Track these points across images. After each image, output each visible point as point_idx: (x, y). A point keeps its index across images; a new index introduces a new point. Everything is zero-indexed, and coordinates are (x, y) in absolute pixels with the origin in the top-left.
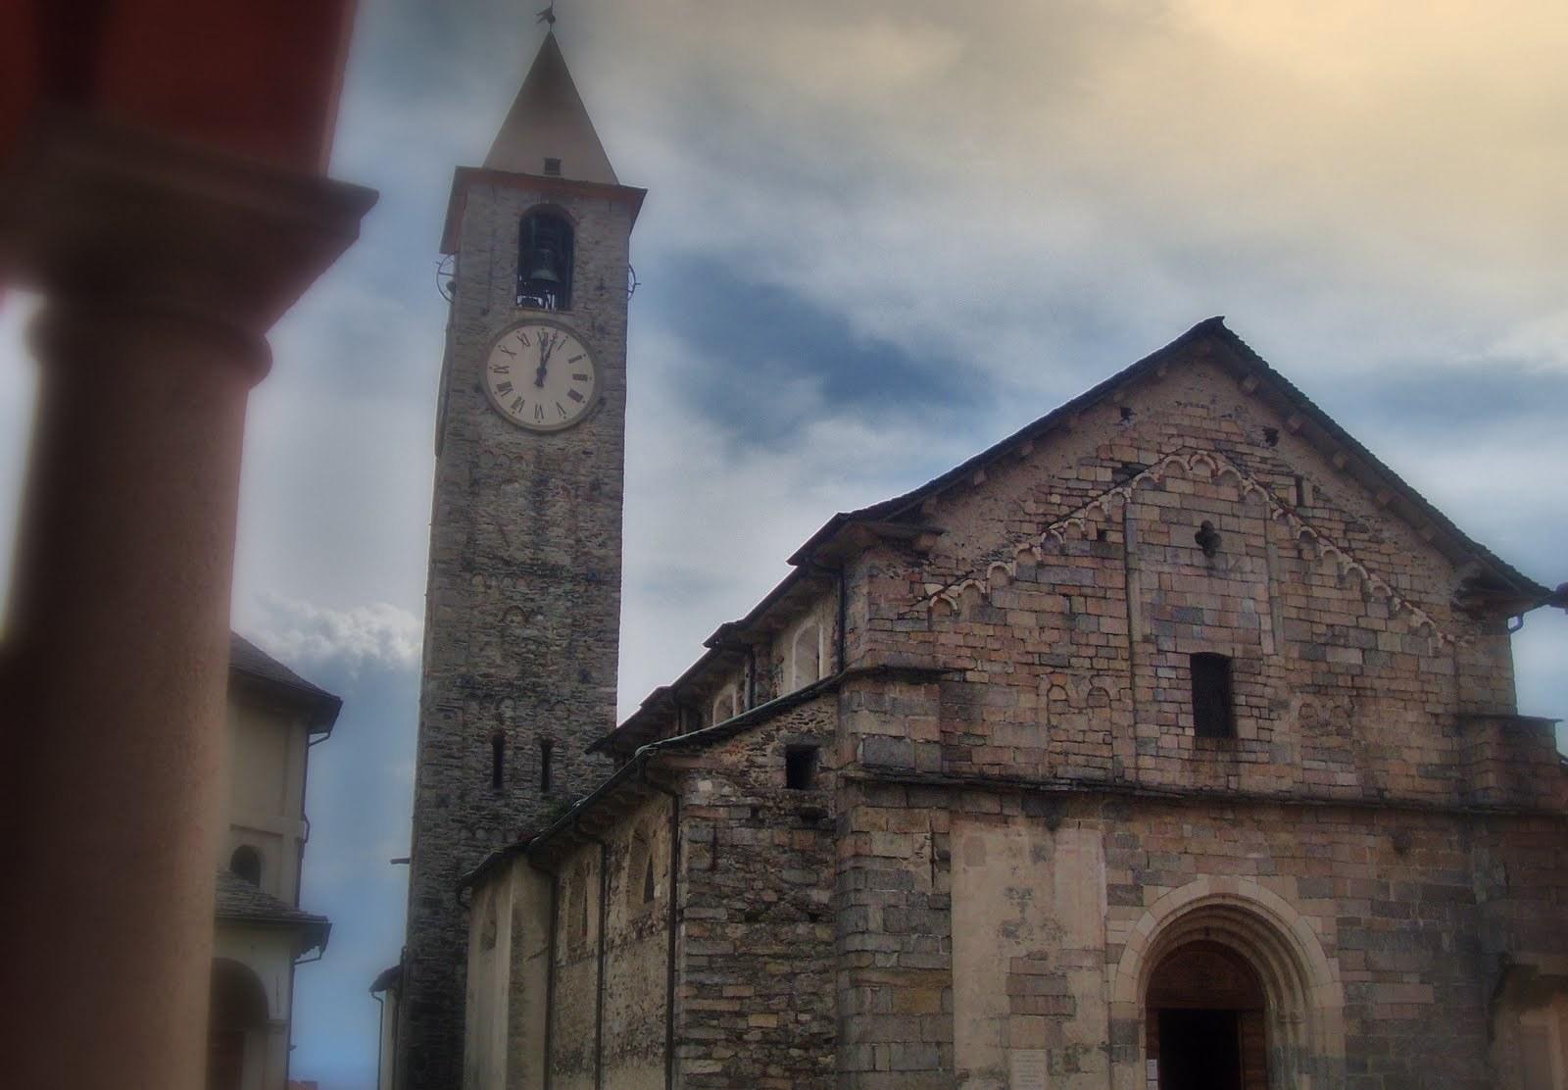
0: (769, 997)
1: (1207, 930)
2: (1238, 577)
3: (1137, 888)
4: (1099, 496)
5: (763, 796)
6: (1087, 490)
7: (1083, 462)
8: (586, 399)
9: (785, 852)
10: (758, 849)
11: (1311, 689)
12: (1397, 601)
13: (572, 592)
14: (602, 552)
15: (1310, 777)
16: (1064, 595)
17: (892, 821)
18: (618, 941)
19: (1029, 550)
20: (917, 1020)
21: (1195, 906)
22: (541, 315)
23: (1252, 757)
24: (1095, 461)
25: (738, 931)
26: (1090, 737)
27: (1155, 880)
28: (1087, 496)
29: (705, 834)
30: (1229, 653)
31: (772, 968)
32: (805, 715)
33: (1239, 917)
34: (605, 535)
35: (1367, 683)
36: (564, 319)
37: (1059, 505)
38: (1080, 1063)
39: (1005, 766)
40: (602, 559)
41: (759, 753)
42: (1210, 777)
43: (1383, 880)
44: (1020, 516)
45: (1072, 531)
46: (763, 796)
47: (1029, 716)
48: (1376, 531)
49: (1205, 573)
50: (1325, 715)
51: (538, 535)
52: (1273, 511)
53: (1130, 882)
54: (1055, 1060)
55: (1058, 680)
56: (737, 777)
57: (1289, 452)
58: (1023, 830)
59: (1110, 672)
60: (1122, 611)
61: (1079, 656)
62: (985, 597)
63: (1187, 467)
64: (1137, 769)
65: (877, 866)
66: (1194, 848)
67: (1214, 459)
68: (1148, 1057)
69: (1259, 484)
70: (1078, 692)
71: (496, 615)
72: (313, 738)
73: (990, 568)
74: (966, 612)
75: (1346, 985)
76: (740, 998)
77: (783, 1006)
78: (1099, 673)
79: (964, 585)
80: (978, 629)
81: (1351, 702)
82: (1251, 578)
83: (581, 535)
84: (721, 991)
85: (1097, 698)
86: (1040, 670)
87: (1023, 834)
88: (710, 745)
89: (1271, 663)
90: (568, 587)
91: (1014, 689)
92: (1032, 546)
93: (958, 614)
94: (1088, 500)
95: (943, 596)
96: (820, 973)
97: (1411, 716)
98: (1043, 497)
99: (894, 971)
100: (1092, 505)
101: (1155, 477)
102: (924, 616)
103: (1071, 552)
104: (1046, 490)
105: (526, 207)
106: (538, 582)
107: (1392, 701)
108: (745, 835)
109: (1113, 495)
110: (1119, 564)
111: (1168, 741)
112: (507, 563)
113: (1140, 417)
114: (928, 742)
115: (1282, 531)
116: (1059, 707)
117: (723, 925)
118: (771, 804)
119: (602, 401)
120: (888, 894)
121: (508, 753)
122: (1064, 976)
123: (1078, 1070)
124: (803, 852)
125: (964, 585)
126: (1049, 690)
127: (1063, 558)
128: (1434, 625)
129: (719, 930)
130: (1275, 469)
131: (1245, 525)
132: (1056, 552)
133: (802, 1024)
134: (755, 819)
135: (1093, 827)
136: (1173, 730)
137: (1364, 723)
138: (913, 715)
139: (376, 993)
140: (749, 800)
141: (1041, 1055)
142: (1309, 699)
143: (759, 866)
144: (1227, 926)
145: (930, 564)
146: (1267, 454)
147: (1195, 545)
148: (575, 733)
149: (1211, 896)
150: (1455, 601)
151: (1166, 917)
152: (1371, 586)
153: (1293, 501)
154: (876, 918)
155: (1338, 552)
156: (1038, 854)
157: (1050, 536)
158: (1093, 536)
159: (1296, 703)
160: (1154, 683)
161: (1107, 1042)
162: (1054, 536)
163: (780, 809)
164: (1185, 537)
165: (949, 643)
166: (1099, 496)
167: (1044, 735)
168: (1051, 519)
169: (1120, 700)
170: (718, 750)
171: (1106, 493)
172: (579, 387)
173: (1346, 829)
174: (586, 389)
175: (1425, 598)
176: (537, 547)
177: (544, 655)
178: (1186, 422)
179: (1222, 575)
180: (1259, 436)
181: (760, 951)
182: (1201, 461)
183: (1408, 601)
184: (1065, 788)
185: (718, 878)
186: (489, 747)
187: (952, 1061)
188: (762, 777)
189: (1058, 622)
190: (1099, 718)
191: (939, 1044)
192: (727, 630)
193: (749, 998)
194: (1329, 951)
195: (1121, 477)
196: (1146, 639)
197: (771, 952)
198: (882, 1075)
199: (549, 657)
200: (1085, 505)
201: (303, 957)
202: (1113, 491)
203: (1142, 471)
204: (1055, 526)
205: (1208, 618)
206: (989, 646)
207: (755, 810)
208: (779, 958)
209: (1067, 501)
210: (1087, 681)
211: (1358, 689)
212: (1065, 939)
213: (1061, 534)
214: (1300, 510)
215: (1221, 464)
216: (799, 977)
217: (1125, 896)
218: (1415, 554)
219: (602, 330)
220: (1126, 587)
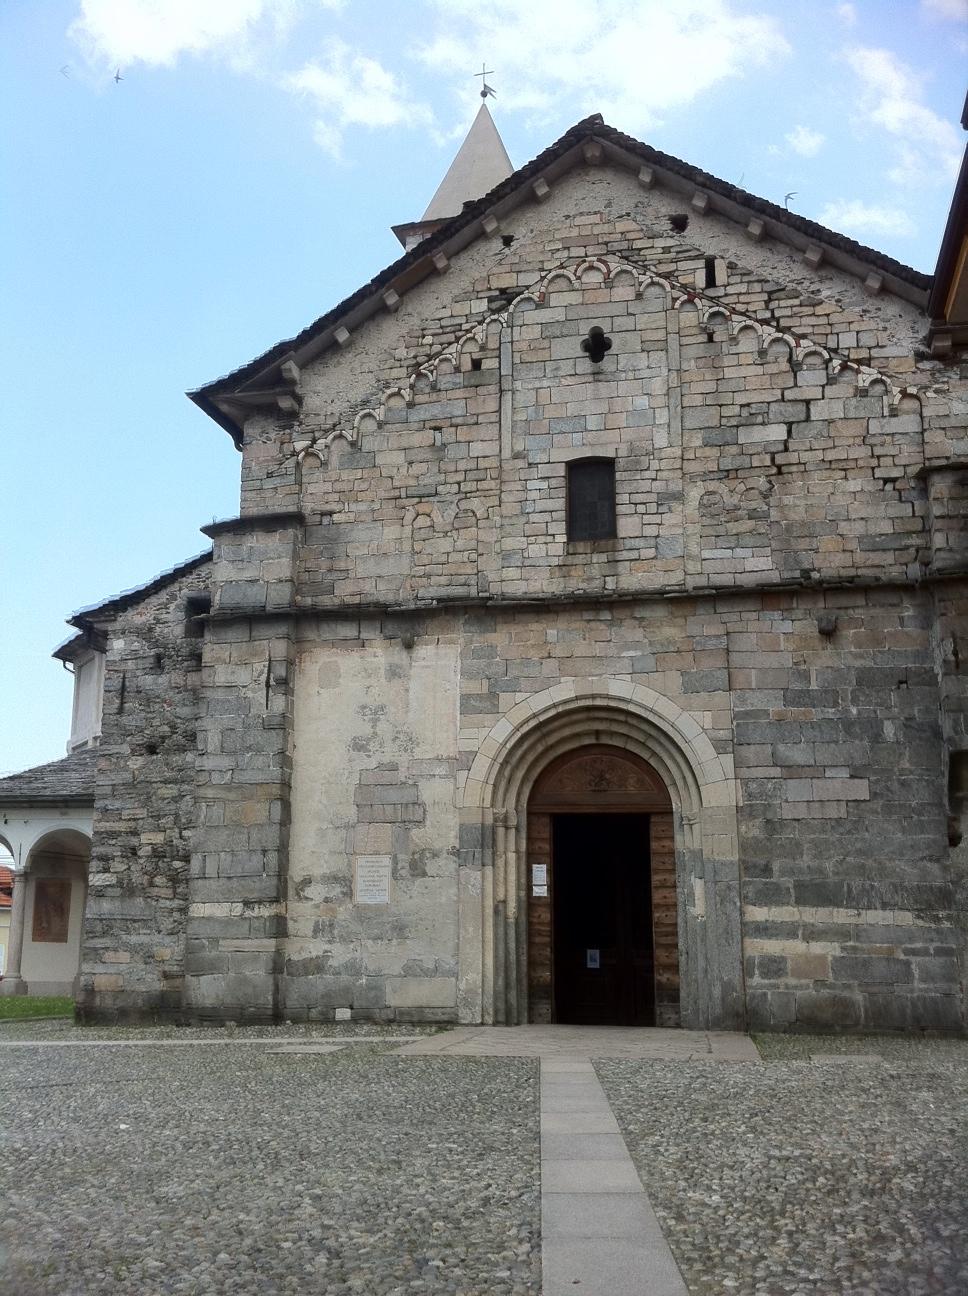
1: (597, 733)
2: (631, 375)
3: (493, 695)
4: (473, 328)
6: (461, 325)
7: (458, 299)
11: (716, 476)
12: (836, 363)
15: (709, 567)
17: (234, 654)
19: (398, 394)
20: (246, 831)
23: (634, 555)
24: (473, 294)
25: (135, 763)
26: (454, 557)
28: (461, 330)
30: (611, 454)
33: (622, 718)
35: (793, 457)
37: (431, 345)
38: (427, 869)
41: (164, 611)
42: (591, 574)
43: (803, 667)
45: (445, 367)
47: (392, 548)
48: (813, 292)
49: (591, 379)
50: (731, 501)
52: (675, 300)
53: (485, 690)
55: (422, 508)
56: (146, 633)
57: (702, 236)
58: (379, 652)
61: (446, 483)
62: (353, 444)
63: (573, 278)
65: (220, 695)
66: (558, 652)
67: (604, 262)
69: (659, 275)
73: (358, 418)
75: (746, 782)
78: (467, 495)
79: (331, 437)
81: (770, 482)
82: (646, 373)
84: (120, 814)
86: (405, 502)
87: (380, 653)
88: (125, 610)
89: (663, 455)
91: (379, 523)
92: (400, 389)
93: (324, 464)
94: (460, 334)
97: (853, 485)
99: (228, 787)
100: (464, 338)
103: (442, 388)
104: (419, 333)
107: (826, 474)
108: (147, 681)
109: (488, 324)
110: (493, 389)
111: (536, 550)
113: (522, 241)
115: (689, 318)
116: (423, 534)
117: (126, 758)
120: (227, 720)
122: (415, 785)
123: (424, 874)
127: (434, 395)
128: (888, 381)
129: (122, 763)
130: (680, 255)
131: (642, 321)
132: (427, 390)
133: (185, 840)
135: (452, 642)
136: (542, 539)
137: (786, 502)
138: (268, 559)
141: (387, 861)
142: (712, 486)
143: (157, 706)
144: (615, 728)
145: (301, 424)
146: (670, 242)
147: (582, 354)
149: (577, 698)
150: (922, 348)
152: (799, 354)
153: (700, 279)
155: (757, 325)
156: (394, 672)
157: (420, 375)
158: (467, 365)
159: (695, 493)
160: (521, 496)
161: (458, 846)
164: (573, 347)
165: (317, 493)
166: (473, 328)
167: (406, 561)
168: (420, 359)
169: (488, 518)
171: (480, 323)
173: (754, 615)
175: (875, 353)
178: (575, 233)
179: (610, 377)
180: (666, 226)
182: (591, 268)
183: (852, 361)
185: (125, 720)
189: (428, 455)
190: (464, 539)
193: (143, 819)
194: (720, 747)
195: (495, 305)
198: (211, 881)
200: (457, 339)
203: (522, 293)
204: (426, 365)
205: (592, 423)
207: (159, 658)
208: (170, 783)
209: (438, 339)
210: (454, 506)
211: (779, 467)
212: (417, 750)
213: (432, 372)
214: (711, 292)
215: (612, 266)
216: (185, 799)
217: (479, 704)
218: (865, 307)
220: (499, 411)
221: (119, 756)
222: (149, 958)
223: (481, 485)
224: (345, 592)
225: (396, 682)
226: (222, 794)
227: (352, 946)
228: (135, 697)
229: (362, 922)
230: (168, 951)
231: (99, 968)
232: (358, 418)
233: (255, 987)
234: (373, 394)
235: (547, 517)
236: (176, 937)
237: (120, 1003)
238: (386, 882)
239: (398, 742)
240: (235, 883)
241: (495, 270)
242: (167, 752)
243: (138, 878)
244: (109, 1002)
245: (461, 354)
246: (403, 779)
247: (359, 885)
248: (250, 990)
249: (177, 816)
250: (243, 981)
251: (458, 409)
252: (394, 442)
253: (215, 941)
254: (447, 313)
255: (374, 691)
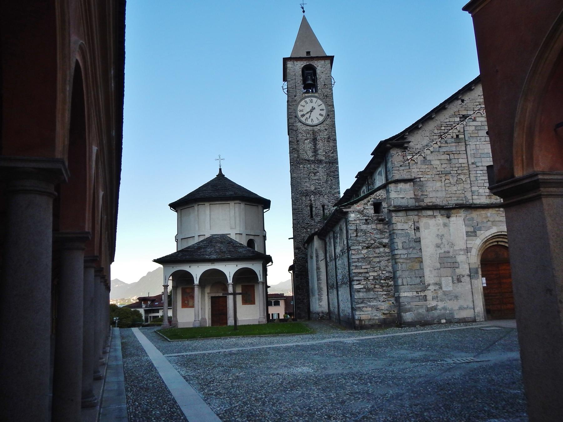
0: (374, 268)
1: (497, 242)
5: (368, 216)
8: (324, 115)
9: (375, 230)
10: (368, 230)
13: (326, 166)
14: (333, 155)
16: (448, 154)
18: (338, 256)
19: (436, 143)
21: (493, 235)
22: (310, 95)
24: (455, 115)
25: (364, 251)
26: (458, 192)
27: (480, 229)
29: (353, 227)
31: (374, 260)
32: (378, 194)
34: (333, 150)
36: (316, 95)
37: (444, 130)
38: (462, 280)
39: (434, 202)
40: (333, 157)
44: (433, 134)
45: (449, 136)
46: (368, 216)
47: (440, 189)
51: (315, 153)
54: (454, 280)
55: (447, 177)
59: (462, 174)
60: (465, 156)
62: (424, 158)
64: (472, 199)
65: (400, 232)
68: (482, 277)
70: (453, 180)
71: (307, 174)
72: (265, 211)
73: (425, 150)
74: (419, 163)
76: (367, 268)
77: (378, 270)
78: (459, 174)
79: (418, 155)
80: (423, 166)
83: (327, 151)
85: (459, 181)
86: (441, 175)
87: (440, 220)
90: (325, 165)
91: (434, 181)
92: (437, 142)
93: (417, 163)
95: (412, 159)
96: (387, 260)
98: (439, 128)
99: (406, 259)
101: (473, 118)
102: (408, 165)
103: (448, 142)
105: (303, 66)
106: (317, 165)
108: (364, 227)
110: (463, 144)
111: (481, 191)
112: (308, 161)
113: (467, 101)
114: (411, 198)
116: (448, 185)
117: (361, 250)
118: (370, 218)
119: (328, 115)
120: (403, 239)
121: (314, 209)
122: (455, 257)
123: (461, 282)
124: (380, 230)
125: (418, 155)
126: (445, 181)
127: (446, 144)
129: (360, 252)
132: (444, 143)
134: (367, 222)
135: (460, 216)
136: (483, 188)
139: (290, 272)
140: (365, 218)
141: (450, 278)
143: (368, 234)
145: (408, 151)
147: (487, 135)
148: (330, 202)
149: (497, 232)
151: (484, 239)
154: (400, 246)
156: (445, 225)
157: (442, 138)
160: (476, 175)
162: (443, 138)
163: (373, 219)
165: (415, 172)
167: (444, 193)
168: (442, 134)
169: (466, 181)
170: (355, 206)
171: (458, 124)
172: (322, 112)
174: (324, 113)
176: (315, 156)
177: (320, 183)
181: (371, 256)
184: (451, 207)
185: (358, 239)
186: (309, 208)
187: (424, 281)
188: (368, 211)
189: (447, 162)
190: (460, 187)
191: (420, 277)
192: (360, 173)
195: (462, 119)
196: (473, 163)
197: (374, 256)
199: (321, 183)
201: (268, 265)
202: (460, 124)
203: (469, 117)
204: (444, 135)
206: (426, 171)
209: (446, 128)
213: (445, 138)
219: (326, 96)
220: (466, 150)
221: (358, 249)
222: (378, 309)
223: (463, 171)
224: (427, 201)
225: (446, 227)
226: (405, 261)
227: (444, 302)
228: (361, 232)
229: (446, 295)
230: (383, 307)
231: (362, 313)
232: (425, 150)
233: (423, 315)
234: (429, 143)
235: (483, 181)
236: (385, 303)
237: (371, 323)
238: (451, 284)
239: (449, 245)
240: (413, 286)
241: (461, 109)
242: (374, 248)
243: (370, 286)
244: (367, 323)
245: (453, 133)
246: (452, 255)
247: (443, 285)
248: (422, 316)
249: (380, 267)
250: (419, 314)
251: (454, 149)
252: (436, 158)
253: (409, 303)
254: (448, 120)
255: (440, 230)
